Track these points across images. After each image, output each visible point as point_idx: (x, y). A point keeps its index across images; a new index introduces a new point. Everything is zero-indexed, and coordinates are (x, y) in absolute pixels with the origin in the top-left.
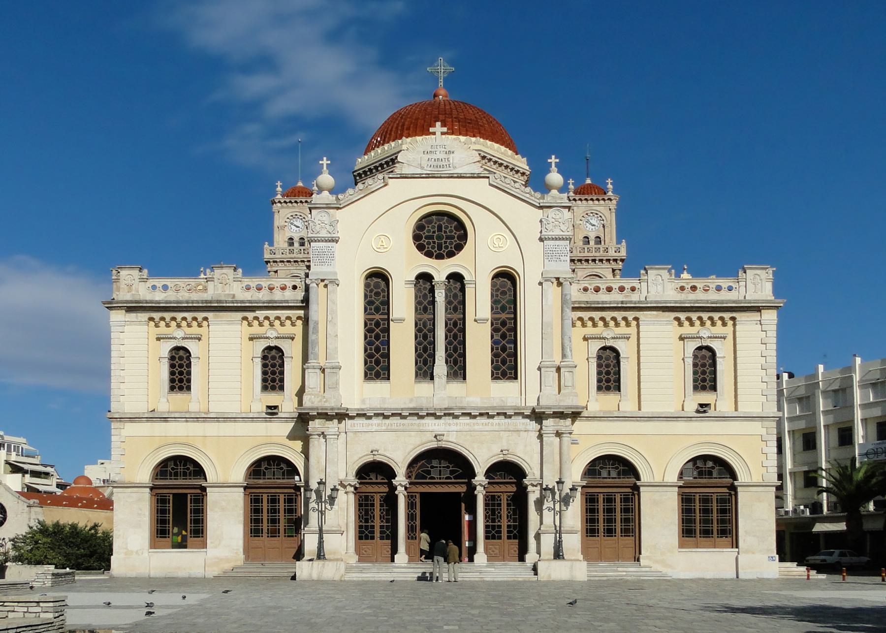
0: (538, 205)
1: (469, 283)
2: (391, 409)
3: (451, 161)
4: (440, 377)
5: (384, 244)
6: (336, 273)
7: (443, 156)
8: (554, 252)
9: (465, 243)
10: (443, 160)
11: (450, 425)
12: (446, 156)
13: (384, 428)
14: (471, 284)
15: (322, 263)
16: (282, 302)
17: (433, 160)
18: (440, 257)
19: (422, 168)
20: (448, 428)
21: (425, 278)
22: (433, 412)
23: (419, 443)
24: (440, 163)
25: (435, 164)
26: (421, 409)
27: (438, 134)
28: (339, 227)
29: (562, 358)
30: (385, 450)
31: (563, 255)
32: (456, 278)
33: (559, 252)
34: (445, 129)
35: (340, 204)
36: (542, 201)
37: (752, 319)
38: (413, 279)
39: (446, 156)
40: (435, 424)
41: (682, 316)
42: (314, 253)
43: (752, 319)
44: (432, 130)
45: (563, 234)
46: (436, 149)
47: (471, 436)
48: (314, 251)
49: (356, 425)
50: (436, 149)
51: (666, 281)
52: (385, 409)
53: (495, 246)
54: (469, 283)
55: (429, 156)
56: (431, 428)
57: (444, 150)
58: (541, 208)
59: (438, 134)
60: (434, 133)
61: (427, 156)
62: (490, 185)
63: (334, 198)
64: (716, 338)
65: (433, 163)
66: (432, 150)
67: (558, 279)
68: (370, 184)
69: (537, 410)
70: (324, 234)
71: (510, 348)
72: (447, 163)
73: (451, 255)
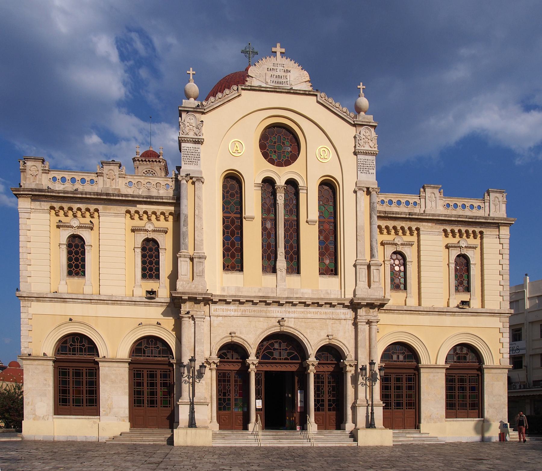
0: (353, 123)
2: (246, 297)
3: (288, 79)
6: (201, 172)
8: (365, 165)
10: (283, 77)
14: (304, 189)
17: (275, 76)
19: (266, 83)
22: (277, 300)
24: (280, 80)
25: (277, 80)
26: (269, 297)
28: (204, 130)
29: (371, 258)
31: (371, 168)
32: (292, 183)
33: (368, 166)
35: (204, 110)
36: (355, 120)
39: (285, 74)
45: (371, 149)
46: (276, 68)
48: (184, 151)
50: (276, 68)
53: (321, 157)
54: (302, 189)
57: (283, 68)
58: (354, 125)
59: (278, 54)
62: (318, 102)
66: (274, 68)
67: (368, 189)
68: (227, 93)
70: (191, 135)
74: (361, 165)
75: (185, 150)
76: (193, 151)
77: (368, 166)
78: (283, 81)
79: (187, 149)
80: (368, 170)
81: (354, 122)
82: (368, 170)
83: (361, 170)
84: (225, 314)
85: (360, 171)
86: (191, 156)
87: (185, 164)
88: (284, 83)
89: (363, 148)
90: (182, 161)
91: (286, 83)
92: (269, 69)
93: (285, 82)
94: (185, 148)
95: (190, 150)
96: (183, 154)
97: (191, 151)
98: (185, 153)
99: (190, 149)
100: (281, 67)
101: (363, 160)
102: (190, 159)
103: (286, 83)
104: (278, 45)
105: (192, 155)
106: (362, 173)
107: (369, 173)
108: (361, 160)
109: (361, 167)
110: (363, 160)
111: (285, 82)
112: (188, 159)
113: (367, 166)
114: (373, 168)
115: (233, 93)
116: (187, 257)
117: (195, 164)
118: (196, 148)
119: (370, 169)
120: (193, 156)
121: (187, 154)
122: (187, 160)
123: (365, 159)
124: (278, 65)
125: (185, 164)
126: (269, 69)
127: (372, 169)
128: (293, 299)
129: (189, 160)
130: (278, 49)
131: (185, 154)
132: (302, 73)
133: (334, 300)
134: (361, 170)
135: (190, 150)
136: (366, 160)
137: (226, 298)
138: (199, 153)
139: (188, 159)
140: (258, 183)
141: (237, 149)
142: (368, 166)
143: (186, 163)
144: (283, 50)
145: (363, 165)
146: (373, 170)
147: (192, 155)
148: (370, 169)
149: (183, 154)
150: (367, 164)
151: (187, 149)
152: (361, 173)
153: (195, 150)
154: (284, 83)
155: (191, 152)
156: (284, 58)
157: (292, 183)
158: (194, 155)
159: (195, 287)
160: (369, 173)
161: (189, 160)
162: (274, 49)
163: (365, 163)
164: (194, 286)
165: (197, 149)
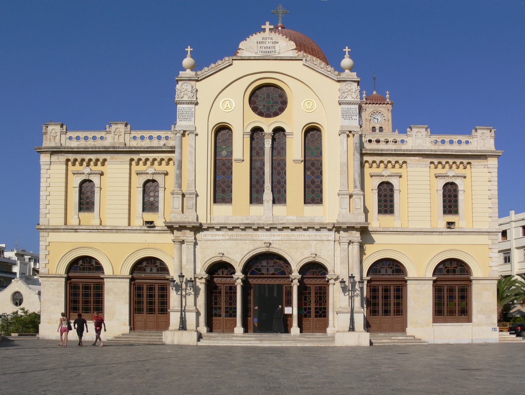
0: (337, 80)
1: (288, 135)
2: (232, 224)
3: (276, 49)
4: (268, 202)
5: (229, 106)
7: (271, 45)
8: (348, 113)
9: (286, 107)
10: (271, 48)
11: (274, 236)
12: (273, 45)
13: (227, 238)
14: (290, 135)
15: (185, 119)
16: (157, 147)
17: (263, 48)
18: (268, 116)
20: (273, 238)
21: (257, 131)
22: (262, 226)
23: (252, 249)
24: (269, 50)
25: (265, 50)
26: (254, 224)
27: (267, 30)
29: (354, 188)
30: (228, 253)
31: (354, 115)
32: (279, 130)
33: (352, 113)
34: (272, 27)
35: (198, 78)
36: (339, 77)
37: (482, 164)
38: (249, 131)
39: (273, 45)
40: (263, 235)
41: (436, 161)
42: (179, 112)
43: (482, 164)
44: (263, 27)
45: (353, 100)
47: (289, 244)
48: (179, 111)
49: (207, 236)
50: (265, 40)
51: (424, 136)
52: (227, 224)
53: (307, 108)
54: (288, 135)
55: (262, 45)
56: (261, 238)
57: (271, 40)
58: (339, 81)
59: (267, 30)
60: (264, 30)
61: (259, 45)
62: (304, 65)
63: (194, 74)
64: (458, 176)
65: (264, 50)
66: (263, 41)
67: (350, 132)
68: (220, 63)
69: (335, 225)
71: (318, 181)
72: (273, 50)
73: (276, 114)
74: (344, 113)
75: (180, 110)
76: (187, 110)
77: (351, 114)
78: (271, 50)
79: (182, 109)
80: (351, 116)
81: (337, 78)
82: (351, 116)
83: (345, 117)
84: (213, 238)
85: (344, 117)
86: (185, 114)
87: (180, 121)
88: (272, 52)
89: (345, 99)
90: (177, 119)
91: (274, 52)
92: (259, 43)
93: (273, 51)
94: (180, 109)
95: (185, 110)
96: (179, 113)
97: (186, 110)
98: (181, 112)
99: (184, 109)
100: (269, 40)
101: (346, 109)
102: (184, 117)
103: (274, 52)
104: (267, 23)
105: (187, 113)
106: (345, 120)
107: (352, 119)
108: (344, 109)
109: (344, 115)
110: (346, 109)
111: (273, 51)
112: (183, 117)
113: (349, 113)
114: (356, 115)
115: (225, 63)
116: (179, 194)
117: (189, 120)
118: (190, 108)
119: (353, 116)
120: (187, 114)
121: (182, 113)
122: (182, 117)
123: (349, 108)
124: (267, 39)
125: (180, 121)
126: (259, 43)
127: (355, 116)
128: (277, 225)
129: (183, 118)
130: (267, 26)
131: (180, 113)
132: (289, 43)
133: (316, 225)
134: (345, 117)
135: (185, 110)
136: (349, 109)
137: (214, 226)
138: (192, 111)
139: (183, 117)
140: (247, 132)
141: (228, 106)
142: (351, 114)
143: (181, 120)
144: (272, 27)
145: (346, 113)
146: (356, 116)
147: (187, 113)
148: (353, 116)
149: (179, 113)
150: (350, 112)
152: (344, 119)
153: (189, 110)
154: (272, 52)
155: (186, 111)
156: (273, 33)
157: (279, 130)
158: (188, 113)
159: (186, 218)
160: (352, 119)
161: (183, 118)
162: (263, 27)
163: (348, 111)
164: (185, 217)
165: (191, 109)
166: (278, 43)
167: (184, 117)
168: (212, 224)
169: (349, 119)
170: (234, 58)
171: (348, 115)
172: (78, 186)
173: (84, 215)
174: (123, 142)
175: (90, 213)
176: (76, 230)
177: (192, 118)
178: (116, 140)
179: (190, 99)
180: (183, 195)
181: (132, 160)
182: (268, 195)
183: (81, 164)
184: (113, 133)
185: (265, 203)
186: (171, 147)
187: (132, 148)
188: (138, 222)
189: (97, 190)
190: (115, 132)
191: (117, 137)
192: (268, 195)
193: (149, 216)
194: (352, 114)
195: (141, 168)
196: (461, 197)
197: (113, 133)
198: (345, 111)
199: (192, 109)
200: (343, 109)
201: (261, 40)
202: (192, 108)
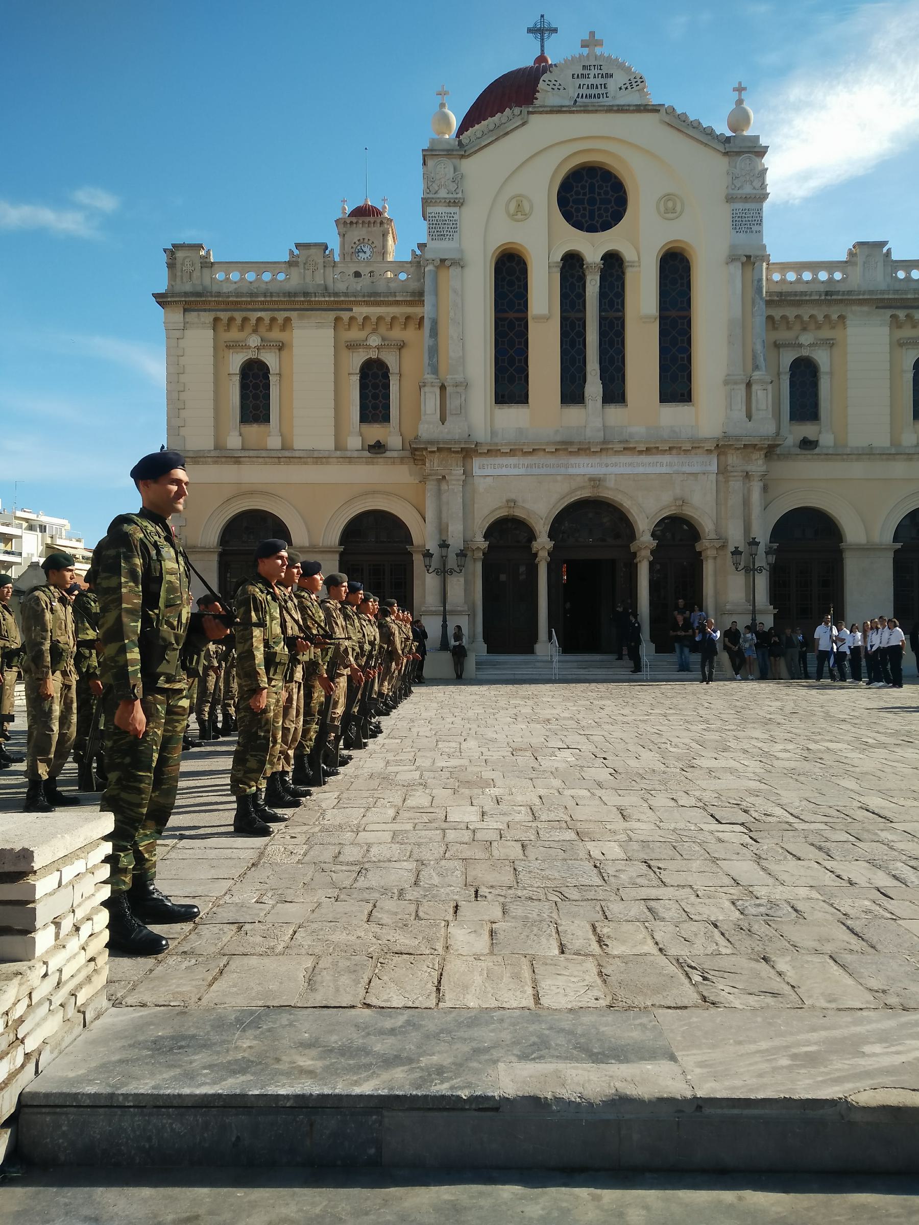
7: (599, 81)
8: (744, 220)
12: (603, 81)
31: (756, 223)
45: (755, 192)
48: (431, 219)
71: (683, 359)
72: (604, 91)
74: (737, 218)
75: (432, 217)
76: (446, 218)
79: (437, 215)
83: (738, 228)
85: (736, 229)
87: (432, 239)
89: (740, 191)
95: (441, 217)
101: (740, 211)
102: (441, 232)
107: (752, 232)
110: (740, 211)
117: (449, 239)
120: (446, 226)
121: (436, 224)
134: (738, 228)
135: (441, 217)
138: (455, 221)
142: (749, 221)
143: (434, 237)
145: (740, 219)
148: (754, 225)
151: (437, 215)
155: (443, 221)
158: (448, 224)
160: (752, 232)
166: (611, 76)
167: (441, 232)
168: (496, 444)
169: (746, 232)
170: (530, 109)
171: (744, 223)
172: (358, 372)
173: (254, 430)
174: (321, 284)
175: (262, 426)
176: (237, 460)
177: (455, 234)
178: (308, 280)
179: (451, 196)
180: (443, 388)
181: (216, 320)
182: (594, 387)
183: (405, 325)
184: (301, 265)
185: (589, 402)
186: (413, 294)
187: (241, 297)
188: (354, 442)
189: (273, 379)
190: (305, 264)
191: (309, 273)
192: (594, 387)
193: (375, 432)
194: (752, 221)
195: (355, 334)
196: (824, 386)
197: (301, 265)
198: (738, 215)
199: (455, 216)
200: (735, 212)
201: (580, 71)
202: (454, 213)
